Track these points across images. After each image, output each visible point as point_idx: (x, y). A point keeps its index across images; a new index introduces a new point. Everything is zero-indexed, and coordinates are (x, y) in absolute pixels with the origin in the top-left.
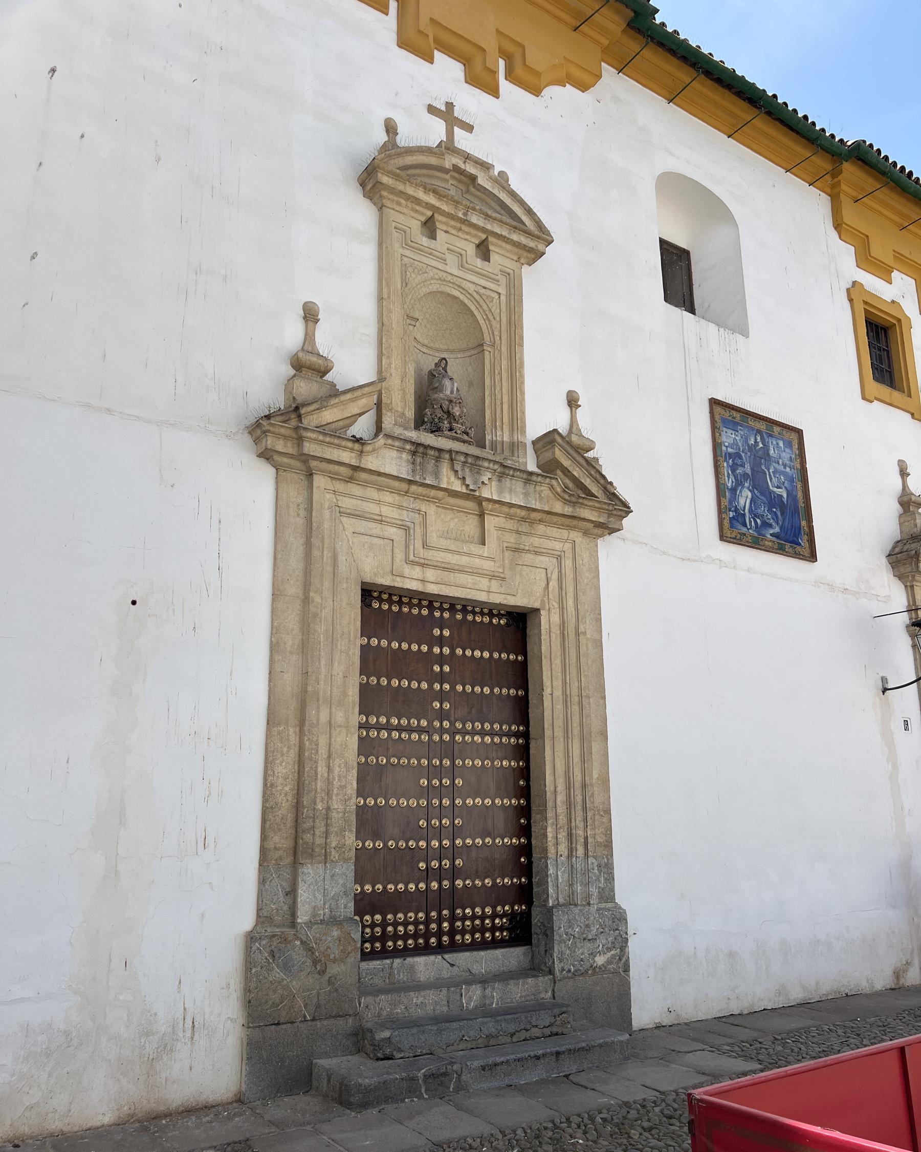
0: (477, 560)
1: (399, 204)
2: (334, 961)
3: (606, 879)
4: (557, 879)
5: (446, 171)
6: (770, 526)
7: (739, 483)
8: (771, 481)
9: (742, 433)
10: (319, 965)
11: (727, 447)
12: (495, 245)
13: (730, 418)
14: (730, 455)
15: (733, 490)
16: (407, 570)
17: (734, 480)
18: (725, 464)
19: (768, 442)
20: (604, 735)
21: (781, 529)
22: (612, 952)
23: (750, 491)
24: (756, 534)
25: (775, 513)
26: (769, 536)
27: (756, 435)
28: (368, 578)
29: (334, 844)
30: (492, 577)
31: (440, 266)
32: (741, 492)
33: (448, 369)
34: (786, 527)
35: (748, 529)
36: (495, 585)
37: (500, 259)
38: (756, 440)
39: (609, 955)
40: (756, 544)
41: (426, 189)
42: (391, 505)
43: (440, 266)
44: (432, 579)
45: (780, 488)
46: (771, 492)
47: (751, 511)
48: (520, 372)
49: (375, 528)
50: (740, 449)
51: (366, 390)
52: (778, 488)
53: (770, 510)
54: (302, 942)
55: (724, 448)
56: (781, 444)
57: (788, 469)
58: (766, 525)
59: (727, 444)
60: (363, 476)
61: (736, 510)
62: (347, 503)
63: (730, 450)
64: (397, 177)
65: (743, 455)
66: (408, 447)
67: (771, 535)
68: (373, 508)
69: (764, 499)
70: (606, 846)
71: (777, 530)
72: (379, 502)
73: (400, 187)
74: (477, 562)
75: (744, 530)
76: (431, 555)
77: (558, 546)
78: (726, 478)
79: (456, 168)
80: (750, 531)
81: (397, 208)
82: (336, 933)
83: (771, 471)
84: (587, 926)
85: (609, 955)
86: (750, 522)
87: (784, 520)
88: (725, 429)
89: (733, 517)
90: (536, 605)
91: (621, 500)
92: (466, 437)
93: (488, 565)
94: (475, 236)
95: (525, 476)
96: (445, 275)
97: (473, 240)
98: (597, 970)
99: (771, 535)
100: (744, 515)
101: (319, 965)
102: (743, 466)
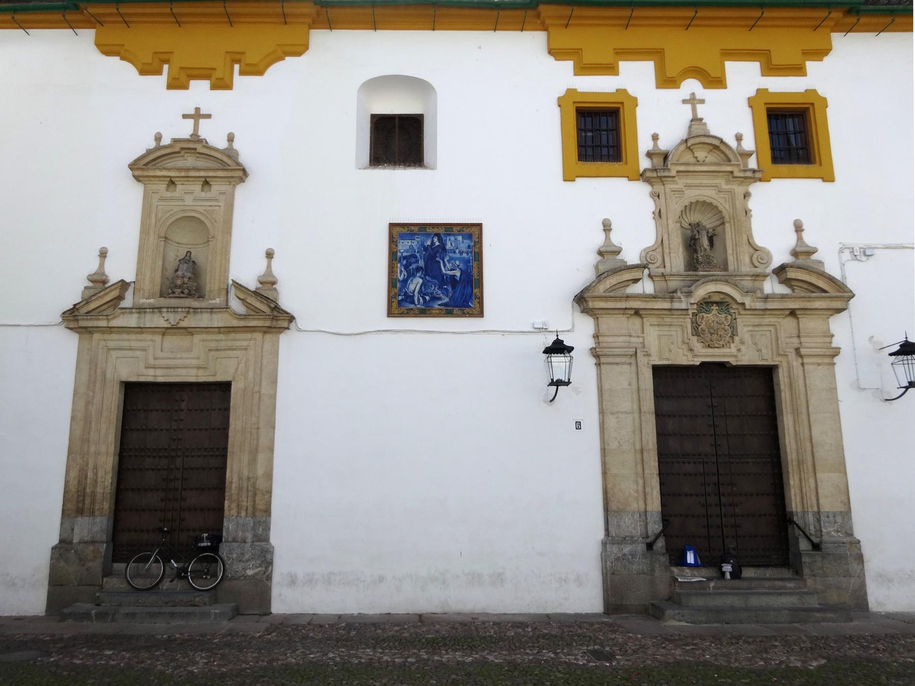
0: (187, 361)
1: (151, 181)
2: (90, 560)
3: (263, 530)
4: (228, 528)
5: (179, 152)
6: (440, 299)
7: (411, 275)
8: (445, 267)
9: (419, 240)
10: (82, 560)
11: (402, 253)
12: (212, 181)
13: (408, 232)
14: (405, 258)
15: (405, 282)
16: (146, 372)
17: (406, 274)
18: (399, 265)
19: (446, 240)
20: (271, 449)
21: (450, 300)
22: (259, 569)
23: (422, 278)
24: (423, 307)
25: (446, 289)
26: (437, 306)
27: (433, 237)
28: (124, 379)
29: (96, 508)
30: (199, 368)
31: (180, 203)
32: (412, 281)
33: (192, 256)
34: (456, 299)
35: (416, 305)
36: (201, 372)
37: (216, 187)
38: (433, 241)
40: (424, 313)
41: (160, 170)
42: (136, 340)
43: (180, 203)
44: (160, 375)
45: (453, 270)
46: (442, 275)
47: (420, 292)
48: (226, 248)
49: (130, 353)
50: (415, 252)
51: (114, 287)
52: (451, 270)
53: (440, 288)
54: (75, 551)
55: (399, 254)
56: (460, 238)
57: (465, 255)
58: (434, 298)
59: (402, 251)
60: (215, 310)
61: (406, 293)
62: (111, 344)
63: (405, 254)
64: (142, 169)
65: (418, 255)
66: (134, 310)
67: (439, 305)
68: (126, 344)
70: (265, 511)
71: (446, 300)
72: (128, 340)
73: (146, 173)
74: (188, 362)
75: (412, 306)
76: (158, 362)
77: (245, 343)
78: (399, 274)
79: (182, 149)
80: (418, 306)
81: (151, 183)
82: (91, 548)
83: (446, 260)
84: (243, 554)
86: (419, 299)
87: (454, 292)
88: (401, 241)
89: (402, 300)
90: (229, 379)
91: (282, 310)
92: (182, 295)
93: (194, 362)
94: (199, 181)
95: (209, 310)
96: (184, 207)
97: (199, 183)
98: (247, 578)
99: (439, 305)
100: (414, 296)
101: (82, 560)
102: (417, 262)
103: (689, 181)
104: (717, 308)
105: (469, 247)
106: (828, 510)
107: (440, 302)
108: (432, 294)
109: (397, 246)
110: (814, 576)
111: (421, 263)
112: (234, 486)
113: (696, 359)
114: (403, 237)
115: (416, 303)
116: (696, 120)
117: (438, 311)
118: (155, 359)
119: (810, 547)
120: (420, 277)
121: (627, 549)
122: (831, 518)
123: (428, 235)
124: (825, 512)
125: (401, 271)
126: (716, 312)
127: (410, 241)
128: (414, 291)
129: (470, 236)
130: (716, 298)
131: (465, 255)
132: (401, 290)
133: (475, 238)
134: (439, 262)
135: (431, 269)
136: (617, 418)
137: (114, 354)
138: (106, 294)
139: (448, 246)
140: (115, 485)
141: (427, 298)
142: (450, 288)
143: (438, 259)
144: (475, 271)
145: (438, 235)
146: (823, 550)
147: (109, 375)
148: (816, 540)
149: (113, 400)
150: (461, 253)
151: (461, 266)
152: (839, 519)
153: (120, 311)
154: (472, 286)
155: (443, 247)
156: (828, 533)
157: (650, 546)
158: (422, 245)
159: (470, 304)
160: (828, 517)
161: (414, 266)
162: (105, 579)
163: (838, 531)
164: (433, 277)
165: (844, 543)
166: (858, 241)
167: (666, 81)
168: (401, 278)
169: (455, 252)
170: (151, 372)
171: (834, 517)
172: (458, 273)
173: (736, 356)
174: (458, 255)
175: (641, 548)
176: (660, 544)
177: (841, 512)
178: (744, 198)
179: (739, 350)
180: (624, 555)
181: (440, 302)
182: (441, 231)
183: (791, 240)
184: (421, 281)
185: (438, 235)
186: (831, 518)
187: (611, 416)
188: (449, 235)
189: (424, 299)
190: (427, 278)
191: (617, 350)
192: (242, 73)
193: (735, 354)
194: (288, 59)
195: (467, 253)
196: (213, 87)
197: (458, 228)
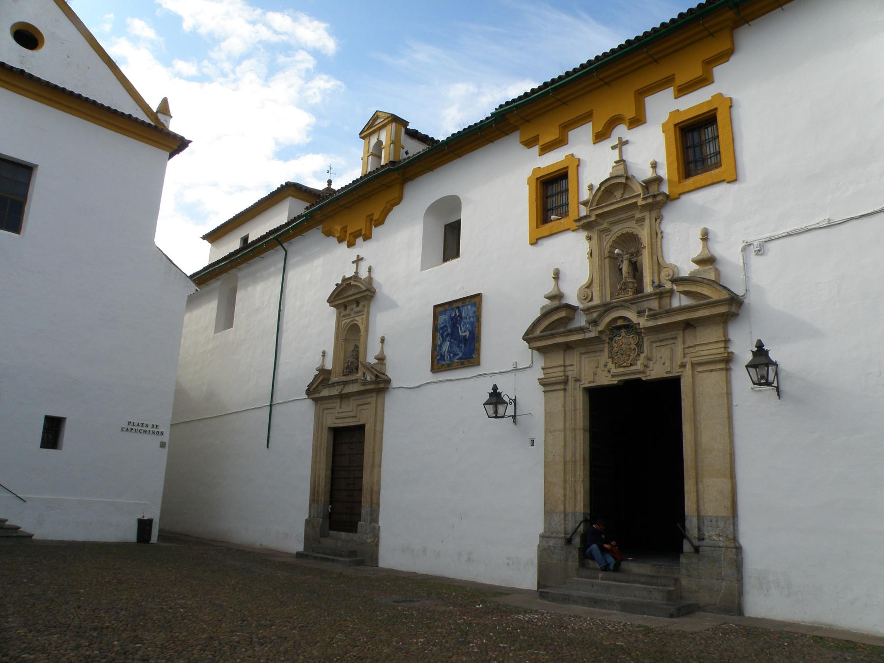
6: (457, 355)
7: (444, 340)
15: (441, 346)
21: (463, 354)
25: (461, 347)
26: (456, 360)
39: (371, 540)
53: (459, 346)
55: (439, 326)
56: (469, 307)
58: (455, 355)
63: (441, 326)
65: (448, 324)
67: (457, 359)
69: (455, 342)
71: (461, 355)
85: (371, 540)
90: (365, 423)
99: (457, 359)
100: (444, 355)
102: (447, 330)
103: (611, 219)
104: (625, 330)
105: (474, 312)
106: (711, 515)
107: (457, 357)
108: (454, 352)
109: (438, 321)
110: (689, 576)
111: (449, 330)
112: (365, 488)
113: (614, 379)
114: (441, 313)
115: (446, 360)
116: (621, 161)
117: (456, 364)
118: (352, 411)
119: (693, 550)
120: (449, 341)
121: (552, 543)
122: (714, 522)
123: (452, 309)
124: (708, 516)
125: (439, 338)
126: (625, 335)
127: (444, 316)
128: (445, 351)
129: (475, 304)
130: (620, 323)
131: (471, 319)
132: (439, 352)
133: (477, 306)
134: (458, 328)
135: (453, 335)
136: (554, 435)
137: (326, 412)
138: (318, 378)
139: (463, 314)
140: (329, 486)
141: (451, 355)
142: (463, 346)
143: (458, 325)
144: (476, 332)
145: (458, 308)
146: (701, 552)
147: (324, 425)
148: (696, 542)
149: (326, 436)
150: (470, 318)
151: (469, 328)
152: (721, 524)
153: (322, 388)
154: (475, 342)
155: (460, 316)
156: (710, 537)
157: (569, 541)
158: (450, 317)
159: (473, 356)
160: (711, 521)
161: (445, 334)
162: (321, 539)
163: (719, 536)
164: (455, 340)
165: (720, 547)
166: (756, 236)
167: (600, 137)
168: (439, 344)
169: (466, 318)
170: (338, 421)
171: (717, 521)
172: (467, 334)
173: (643, 372)
174: (468, 320)
175: (561, 543)
176: (577, 540)
177: (723, 517)
178: (656, 220)
179: (646, 366)
180: (549, 546)
181: (457, 357)
182: (460, 304)
183: (697, 249)
184: (448, 343)
185: (458, 308)
186: (714, 522)
187: (550, 434)
188: (464, 306)
189: (450, 355)
190: (452, 341)
191: (552, 379)
192: (375, 227)
193: (642, 369)
194: (395, 208)
195: (473, 317)
196: (365, 240)
197: (469, 300)
